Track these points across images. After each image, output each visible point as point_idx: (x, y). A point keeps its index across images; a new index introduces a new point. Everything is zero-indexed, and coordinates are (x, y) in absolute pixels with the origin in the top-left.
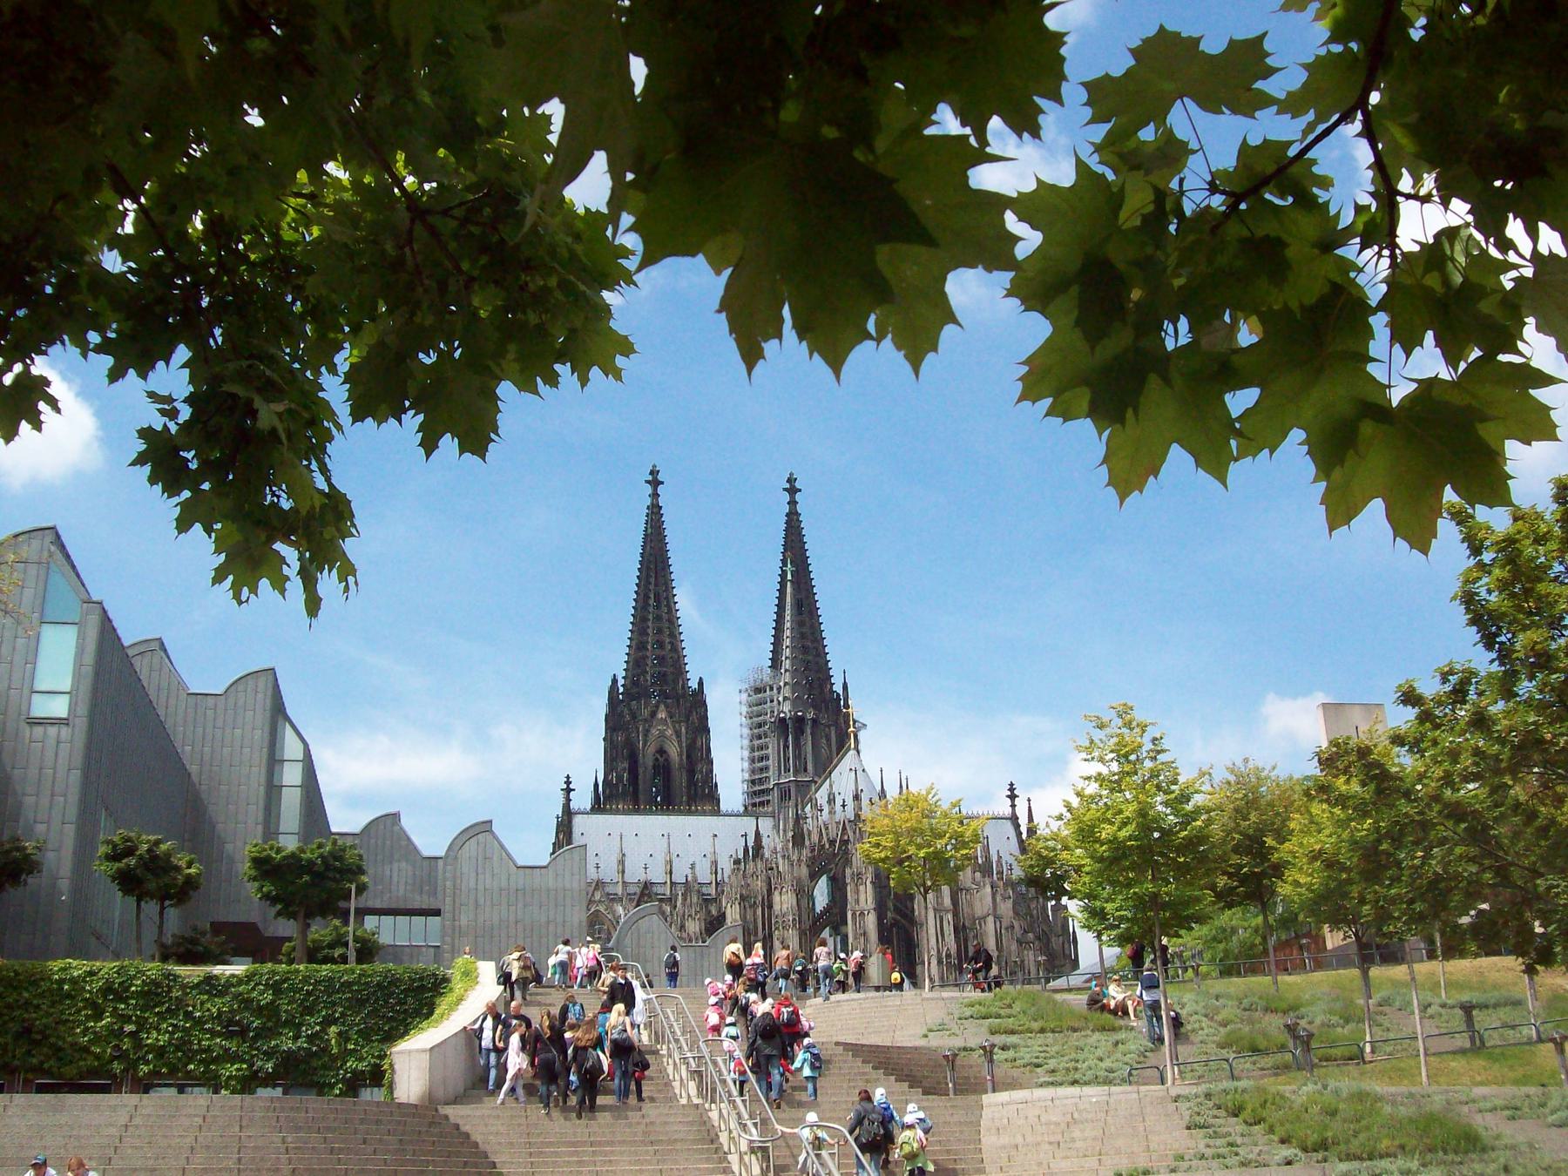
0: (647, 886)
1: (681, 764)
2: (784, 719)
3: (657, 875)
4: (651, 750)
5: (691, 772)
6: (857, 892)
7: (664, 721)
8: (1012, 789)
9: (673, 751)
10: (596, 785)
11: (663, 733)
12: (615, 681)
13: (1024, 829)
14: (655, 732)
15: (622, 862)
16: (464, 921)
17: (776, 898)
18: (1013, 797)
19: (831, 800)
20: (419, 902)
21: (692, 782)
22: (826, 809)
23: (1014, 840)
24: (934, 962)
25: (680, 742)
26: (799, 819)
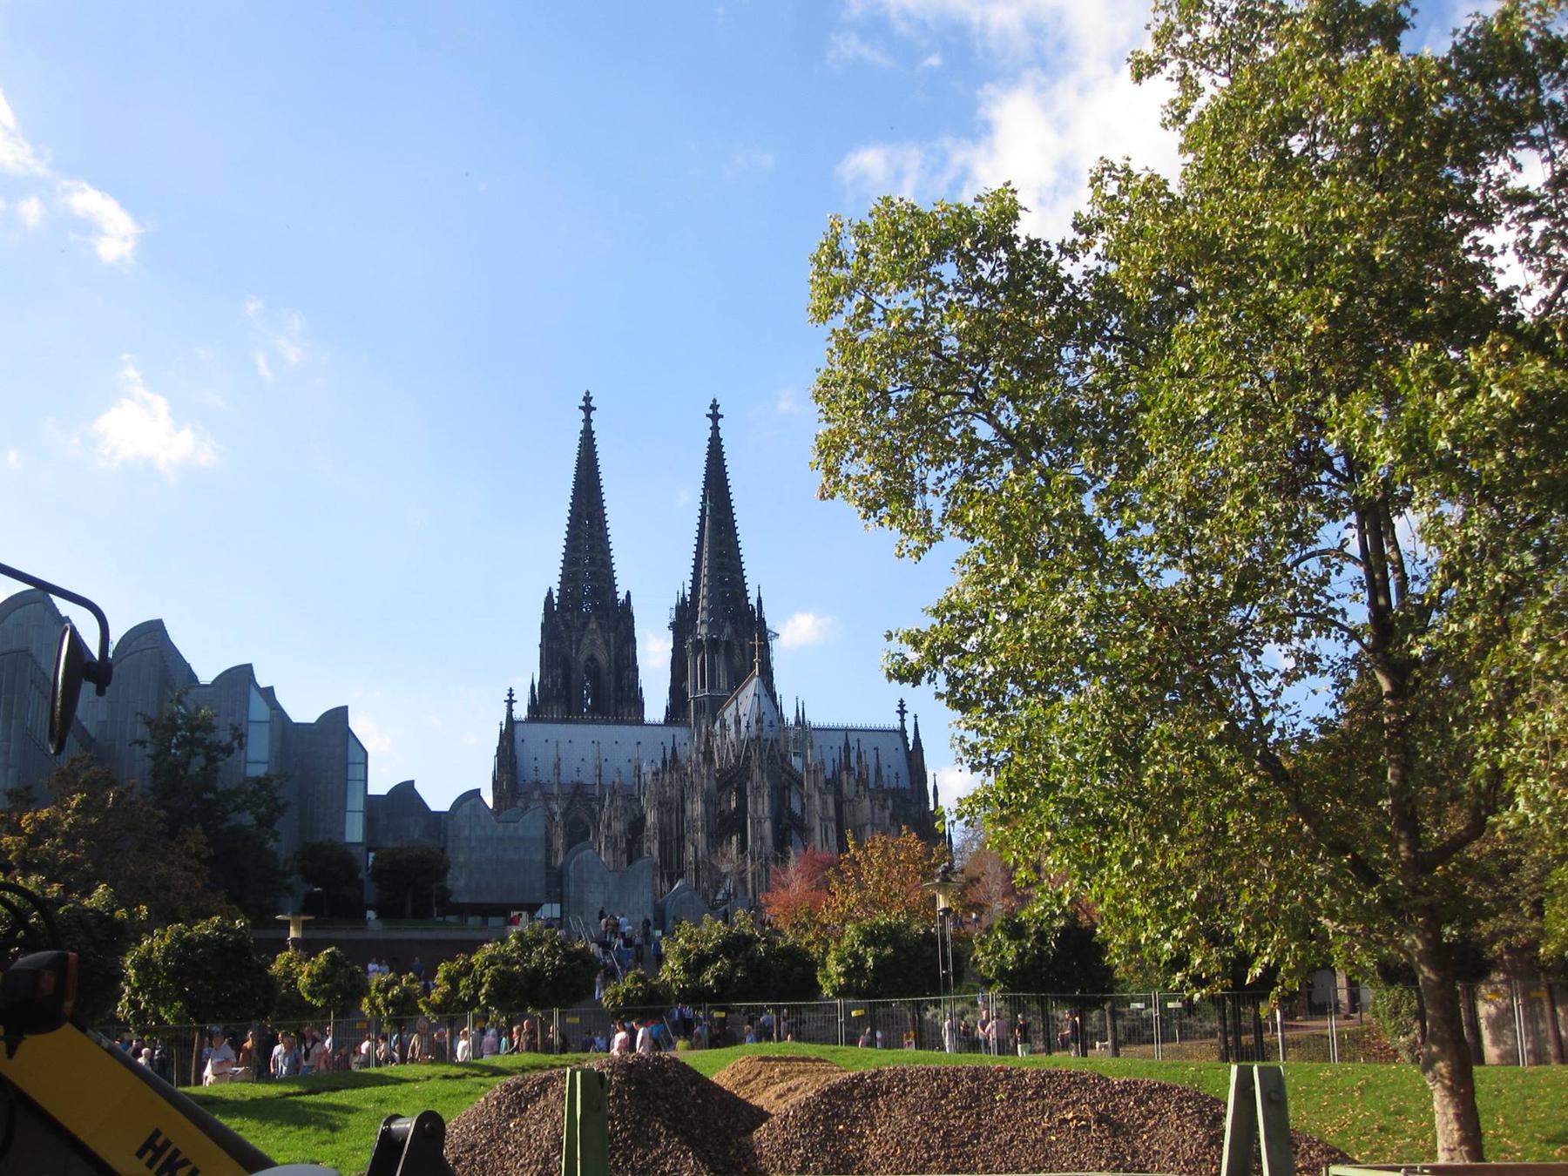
0: (579, 786)
3: (588, 777)
4: (583, 657)
6: (756, 803)
7: (595, 632)
8: (902, 704)
9: (603, 658)
11: (593, 645)
13: (910, 742)
14: (586, 641)
15: (557, 766)
16: (462, 858)
17: (688, 806)
18: (902, 712)
19: (738, 721)
22: (733, 728)
23: (901, 754)
25: (609, 651)
26: (709, 734)
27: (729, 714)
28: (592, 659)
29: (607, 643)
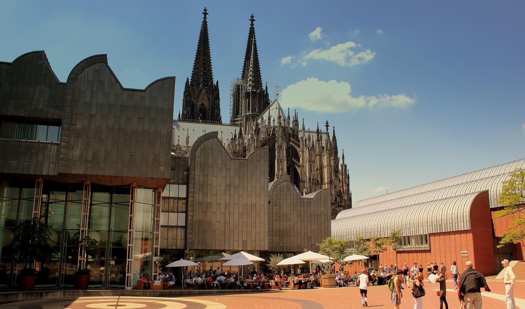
1: (209, 110)
2: (249, 92)
4: (199, 104)
5: (213, 112)
7: (204, 94)
9: (207, 104)
10: (179, 115)
12: (188, 80)
14: (201, 98)
16: (79, 126)
18: (327, 126)
19: (269, 119)
20: (53, 113)
21: (212, 116)
24: (308, 181)
25: (209, 102)
27: (265, 116)
28: (203, 105)
29: (209, 99)
